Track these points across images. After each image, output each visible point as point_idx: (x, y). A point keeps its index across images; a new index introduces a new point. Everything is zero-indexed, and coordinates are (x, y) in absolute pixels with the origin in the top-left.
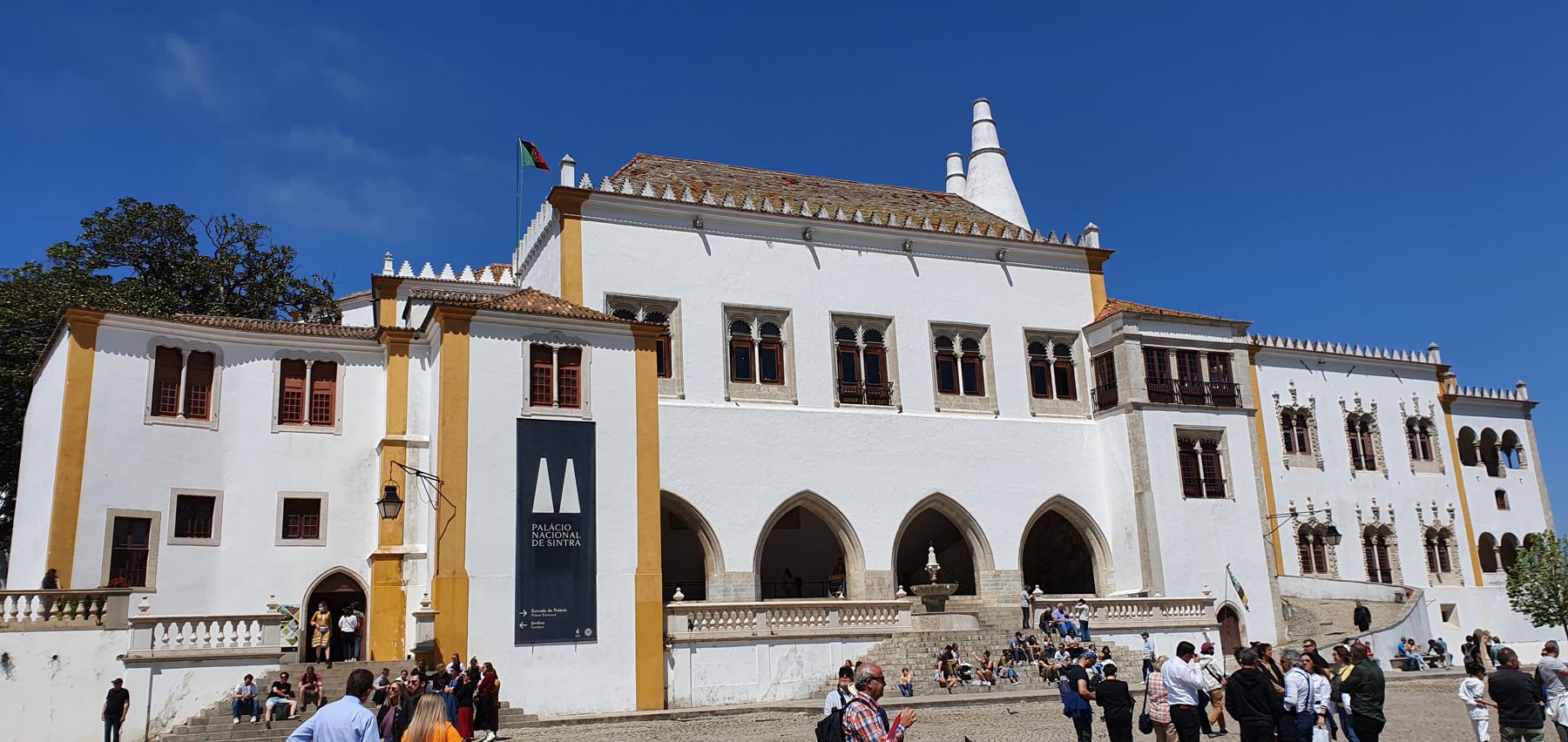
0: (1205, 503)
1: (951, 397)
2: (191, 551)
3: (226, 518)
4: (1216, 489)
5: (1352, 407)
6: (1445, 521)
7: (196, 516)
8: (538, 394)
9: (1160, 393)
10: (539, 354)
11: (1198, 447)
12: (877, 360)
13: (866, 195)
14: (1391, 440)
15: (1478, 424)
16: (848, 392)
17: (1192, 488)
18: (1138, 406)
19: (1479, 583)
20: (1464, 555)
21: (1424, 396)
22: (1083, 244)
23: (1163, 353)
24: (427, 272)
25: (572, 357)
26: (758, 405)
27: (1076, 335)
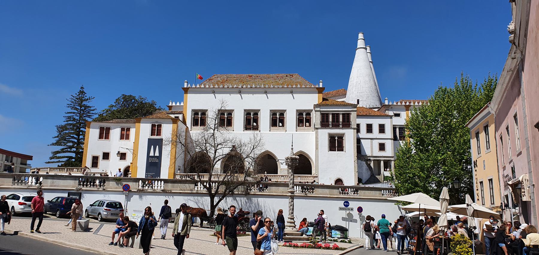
0: (336, 152)
1: (274, 128)
2: (105, 161)
3: (111, 156)
4: (341, 148)
7: (106, 156)
8: (152, 134)
10: (153, 126)
11: (336, 138)
12: (256, 120)
13: (269, 78)
17: (332, 148)
18: (317, 129)
22: (317, 86)
24: (178, 104)
25: (160, 126)
27: (312, 110)
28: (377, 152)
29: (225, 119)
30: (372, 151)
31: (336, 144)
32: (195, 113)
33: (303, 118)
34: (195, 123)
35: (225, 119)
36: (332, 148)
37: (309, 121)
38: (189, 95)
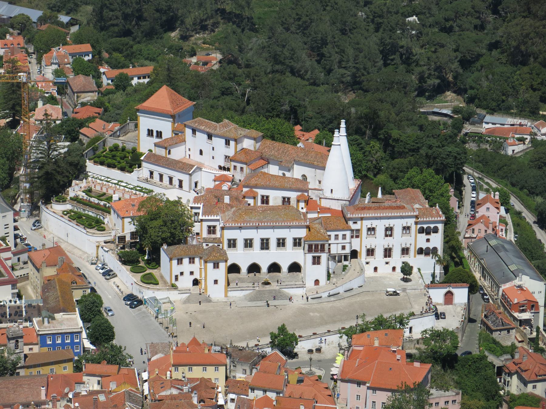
4: (319, 263)
5: (387, 226)
6: (408, 246)
7: (182, 274)
9: (310, 250)
12: (267, 244)
14: (398, 231)
15: (425, 226)
16: (262, 248)
17: (314, 263)
19: (415, 256)
20: (412, 252)
21: (411, 222)
23: (312, 245)
25: (218, 264)
26: (249, 251)
28: (341, 251)
29: (248, 243)
30: (337, 251)
31: (316, 261)
32: (229, 240)
33: (297, 242)
34: (229, 246)
35: (248, 243)
36: (314, 263)
37: (300, 245)
38: (225, 231)
